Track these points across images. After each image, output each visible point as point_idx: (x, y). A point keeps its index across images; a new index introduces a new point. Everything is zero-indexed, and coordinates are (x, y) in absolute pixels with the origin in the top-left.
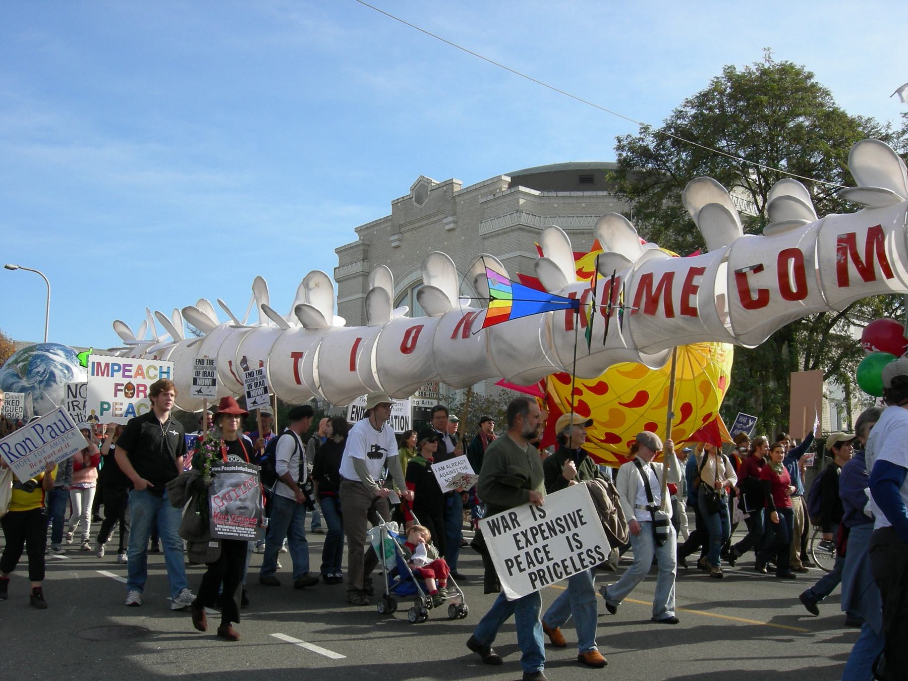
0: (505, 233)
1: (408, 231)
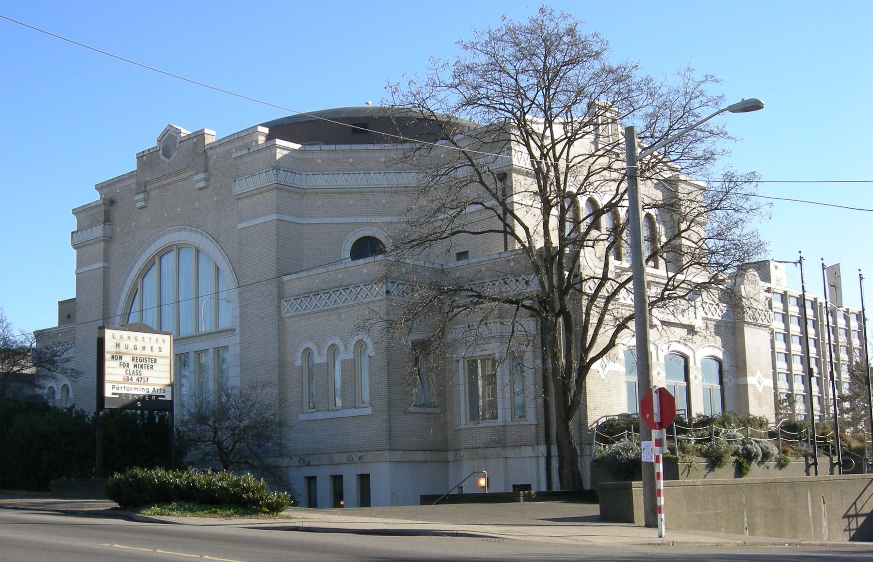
0: (261, 193)
1: (155, 189)
